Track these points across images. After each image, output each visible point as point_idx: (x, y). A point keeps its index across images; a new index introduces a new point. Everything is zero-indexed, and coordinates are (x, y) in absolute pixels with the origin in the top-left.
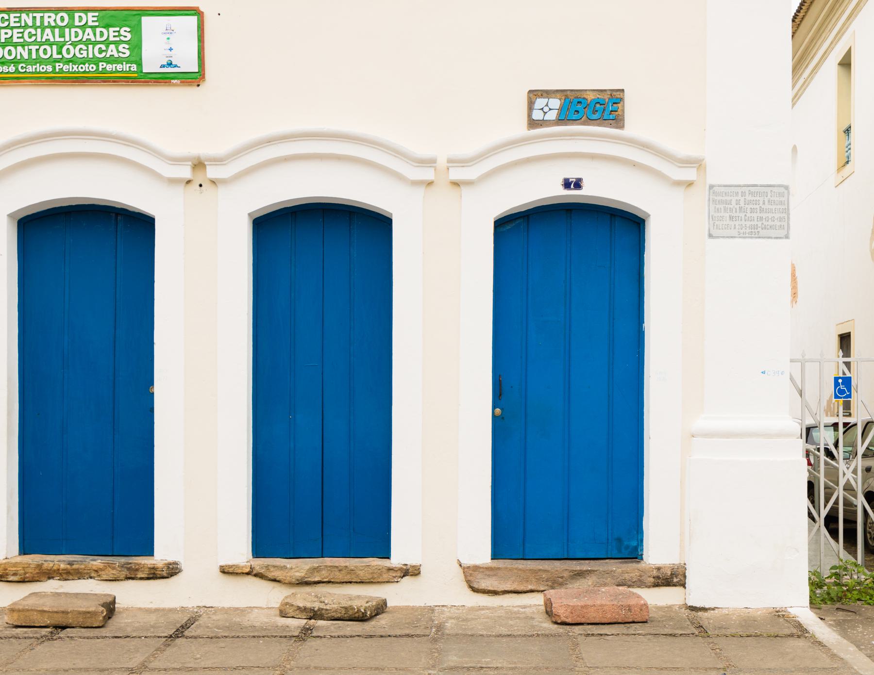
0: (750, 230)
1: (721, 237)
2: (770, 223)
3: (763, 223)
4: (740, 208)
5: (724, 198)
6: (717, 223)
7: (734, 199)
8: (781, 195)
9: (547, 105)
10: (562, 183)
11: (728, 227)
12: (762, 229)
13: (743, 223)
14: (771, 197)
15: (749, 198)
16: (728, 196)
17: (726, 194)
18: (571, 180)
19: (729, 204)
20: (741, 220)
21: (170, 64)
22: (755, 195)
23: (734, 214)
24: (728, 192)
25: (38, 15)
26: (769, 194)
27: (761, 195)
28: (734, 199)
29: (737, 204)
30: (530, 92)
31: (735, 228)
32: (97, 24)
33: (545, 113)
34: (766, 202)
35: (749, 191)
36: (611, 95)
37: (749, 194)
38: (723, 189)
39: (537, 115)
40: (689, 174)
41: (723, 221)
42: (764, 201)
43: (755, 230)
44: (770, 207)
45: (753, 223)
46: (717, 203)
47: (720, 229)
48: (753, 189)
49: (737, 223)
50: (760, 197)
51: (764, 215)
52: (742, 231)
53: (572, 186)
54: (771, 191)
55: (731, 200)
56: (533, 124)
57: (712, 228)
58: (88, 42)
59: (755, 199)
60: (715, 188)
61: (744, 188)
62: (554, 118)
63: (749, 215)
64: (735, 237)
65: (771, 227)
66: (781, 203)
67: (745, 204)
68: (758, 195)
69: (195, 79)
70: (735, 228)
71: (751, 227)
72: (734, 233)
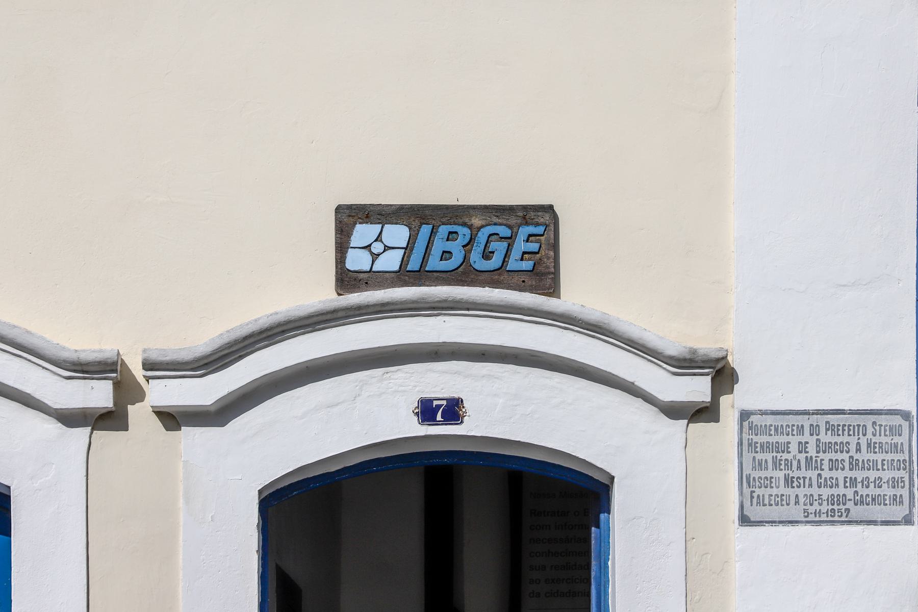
0: (830, 507)
1: (767, 522)
2: (872, 491)
3: (856, 492)
4: (809, 460)
5: (774, 439)
6: (758, 491)
7: (794, 441)
8: (895, 431)
9: (379, 239)
10: (417, 411)
11: (782, 500)
12: (856, 504)
13: (815, 491)
14: (874, 435)
15: (826, 438)
16: (782, 433)
17: (776, 430)
18: (435, 403)
19: (783, 452)
20: (810, 485)
22: (840, 432)
23: (796, 474)
24: (782, 425)
26: (870, 430)
27: (851, 433)
28: (794, 441)
29: (800, 452)
31: (797, 503)
33: (375, 257)
34: (864, 447)
35: (827, 422)
36: (524, 217)
37: (827, 430)
38: (769, 420)
39: (357, 261)
41: (772, 487)
42: (858, 444)
43: (841, 507)
44: (872, 456)
45: (835, 491)
46: (758, 449)
47: (764, 505)
48: (834, 419)
49: (801, 492)
50: (849, 435)
52: (811, 509)
53: (439, 417)
54: (874, 423)
55: (789, 443)
57: (747, 503)
59: (839, 439)
60: (753, 418)
61: (815, 416)
62: (396, 267)
63: (826, 474)
64: (797, 522)
65: (873, 500)
66: (895, 448)
67: (818, 452)
68: (846, 433)
70: (797, 503)
71: (832, 500)
72: (796, 512)
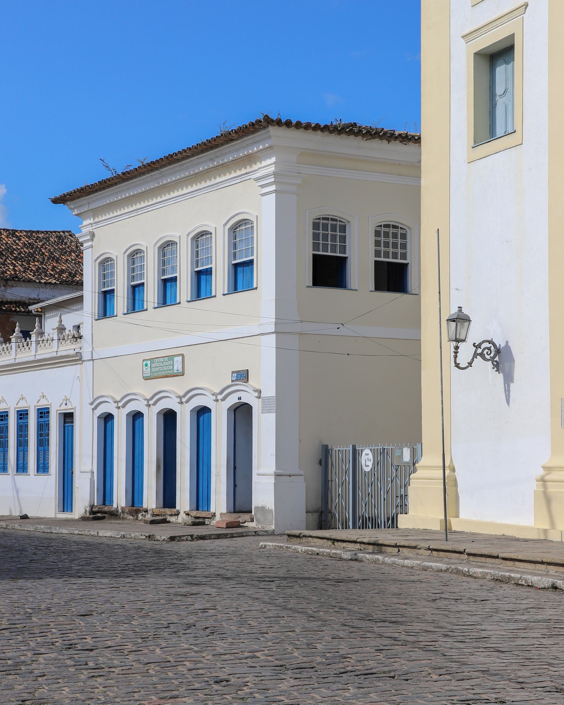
8: (274, 399)
15: (268, 401)
21: (178, 370)
28: (266, 401)
40: (256, 394)
51: (271, 406)
56: (232, 381)
58: (166, 365)
66: (274, 402)
69: (183, 374)
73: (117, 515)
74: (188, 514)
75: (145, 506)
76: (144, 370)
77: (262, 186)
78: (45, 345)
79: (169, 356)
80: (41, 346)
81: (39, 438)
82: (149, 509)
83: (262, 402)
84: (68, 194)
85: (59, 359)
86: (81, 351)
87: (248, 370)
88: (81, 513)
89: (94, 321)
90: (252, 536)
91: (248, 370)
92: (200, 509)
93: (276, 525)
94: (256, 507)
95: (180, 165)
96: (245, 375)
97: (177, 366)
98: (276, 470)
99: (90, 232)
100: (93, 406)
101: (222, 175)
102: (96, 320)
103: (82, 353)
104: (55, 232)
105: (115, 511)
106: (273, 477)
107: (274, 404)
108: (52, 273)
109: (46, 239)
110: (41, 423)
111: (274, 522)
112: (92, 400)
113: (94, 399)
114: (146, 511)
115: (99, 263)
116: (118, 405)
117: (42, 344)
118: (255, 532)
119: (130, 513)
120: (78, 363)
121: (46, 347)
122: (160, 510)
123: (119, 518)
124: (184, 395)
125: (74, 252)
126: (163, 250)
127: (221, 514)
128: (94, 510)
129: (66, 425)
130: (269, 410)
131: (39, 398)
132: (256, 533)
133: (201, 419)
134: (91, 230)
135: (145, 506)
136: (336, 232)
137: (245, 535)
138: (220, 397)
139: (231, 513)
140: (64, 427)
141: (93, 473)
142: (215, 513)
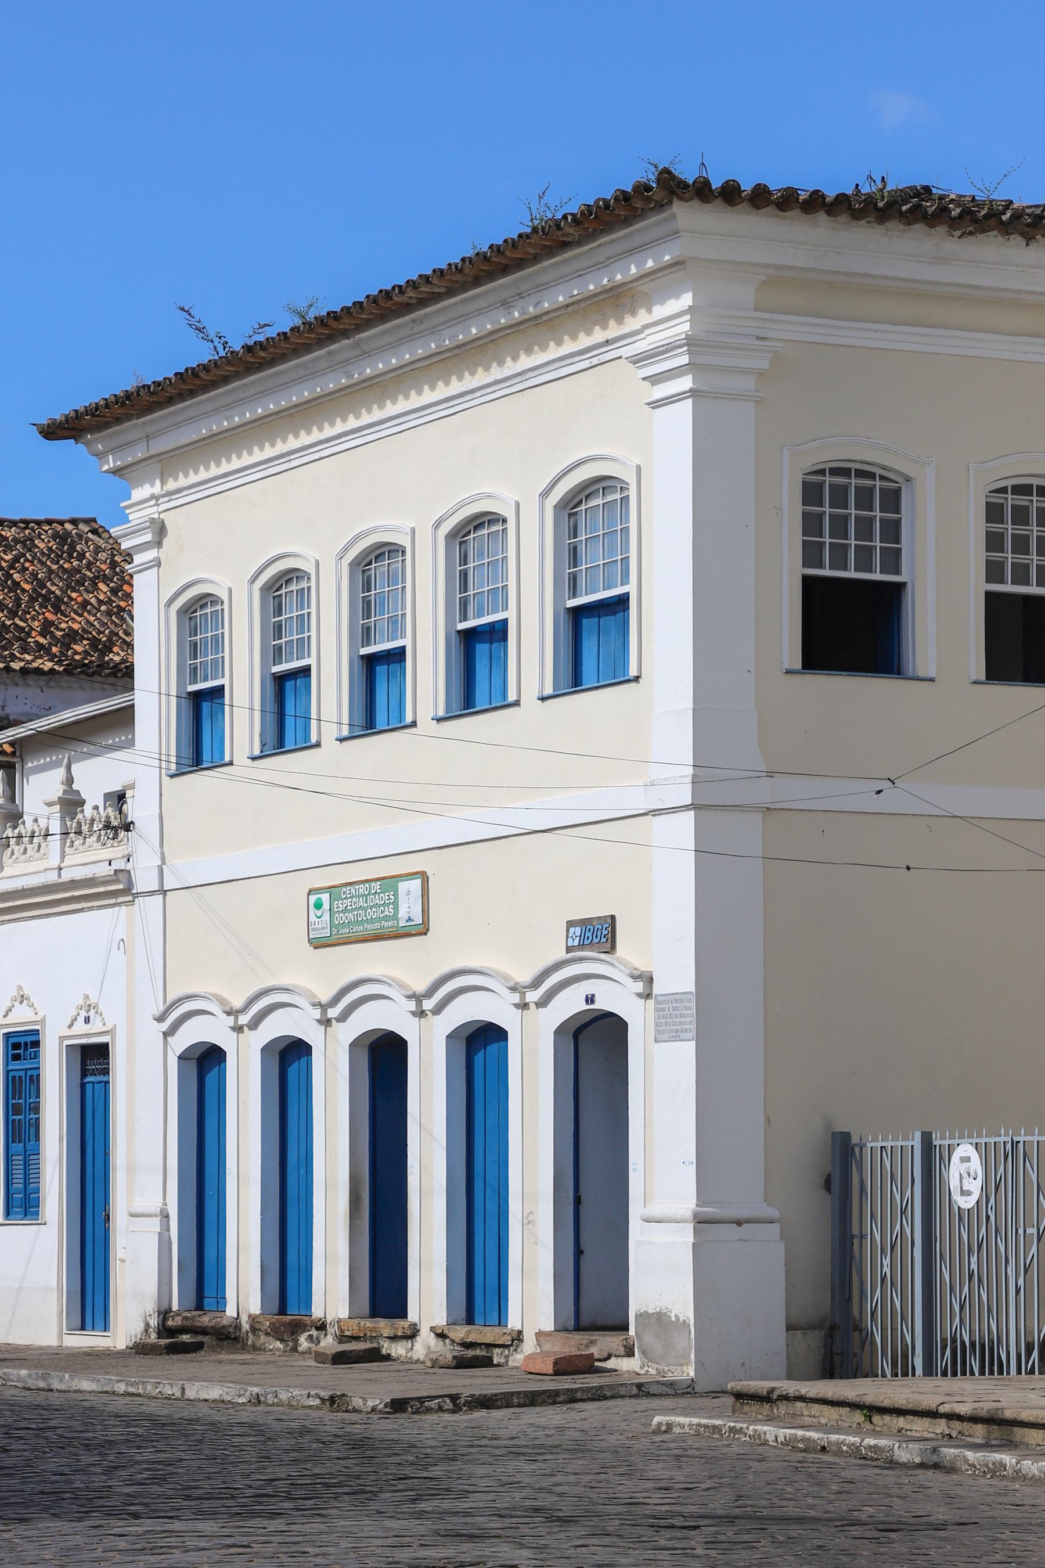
8: (690, 1000)
15: (675, 1005)
21: (410, 919)
25: (357, 887)
28: (667, 1006)
30: (568, 922)
32: (380, 891)
40: (639, 987)
51: (682, 1020)
56: (569, 949)
58: (376, 905)
66: (690, 1008)
73: (236, 1339)
74: (441, 1336)
75: (317, 1312)
76: (312, 918)
77: (654, 380)
78: (26, 849)
79: (384, 878)
80: (12, 853)
81: (11, 1118)
82: (328, 1321)
83: (657, 1010)
84: (88, 411)
85: (66, 890)
86: (129, 866)
87: (613, 917)
88: (133, 1333)
89: (166, 780)
90: (631, 1397)
91: (613, 917)
92: (479, 1319)
93: (700, 1365)
94: (641, 1314)
95: (414, 321)
96: (605, 932)
97: (409, 908)
98: (697, 1205)
99: (152, 521)
100: (165, 1026)
101: (536, 348)
102: (172, 776)
103: (132, 872)
104: (50, 522)
105: (230, 1326)
106: (690, 1227)
107: (691, 1016)
108: (42, 640)
109: (23, 543)
110: (17, 1074)
111: (693, 1357)
112: (162, 1008)
113: (169, 1001)
114: (322, 1327)
115: (178, 611)
116: (236, 1020)
117: (16, 848)
118: (639, 1386)
119: (276, 1332)
120: (121, 900)
121: (28, 854)
122: (362, 1323)
123: (244, 1348)
124: (427, 991)
125: (106, 579)
126: (364, 571)
127: (540, 1335)
128: (170, 1323)
129: (85, 1080)
130: (677, 1031)
131: (10, 1005)
132: (640, 1390)
133: (479, 1058)
134: (156, 516)
135: (317, 1312)
136: (872, 511)
137: (608, 1393)
138: (532, 996)
139: (566, 1330)
140: (83, 1086)
141: (167, 1216)
142: (520, 1332)
